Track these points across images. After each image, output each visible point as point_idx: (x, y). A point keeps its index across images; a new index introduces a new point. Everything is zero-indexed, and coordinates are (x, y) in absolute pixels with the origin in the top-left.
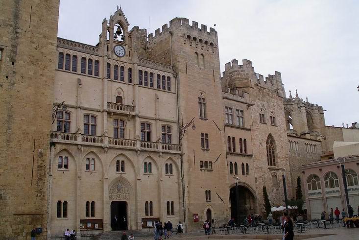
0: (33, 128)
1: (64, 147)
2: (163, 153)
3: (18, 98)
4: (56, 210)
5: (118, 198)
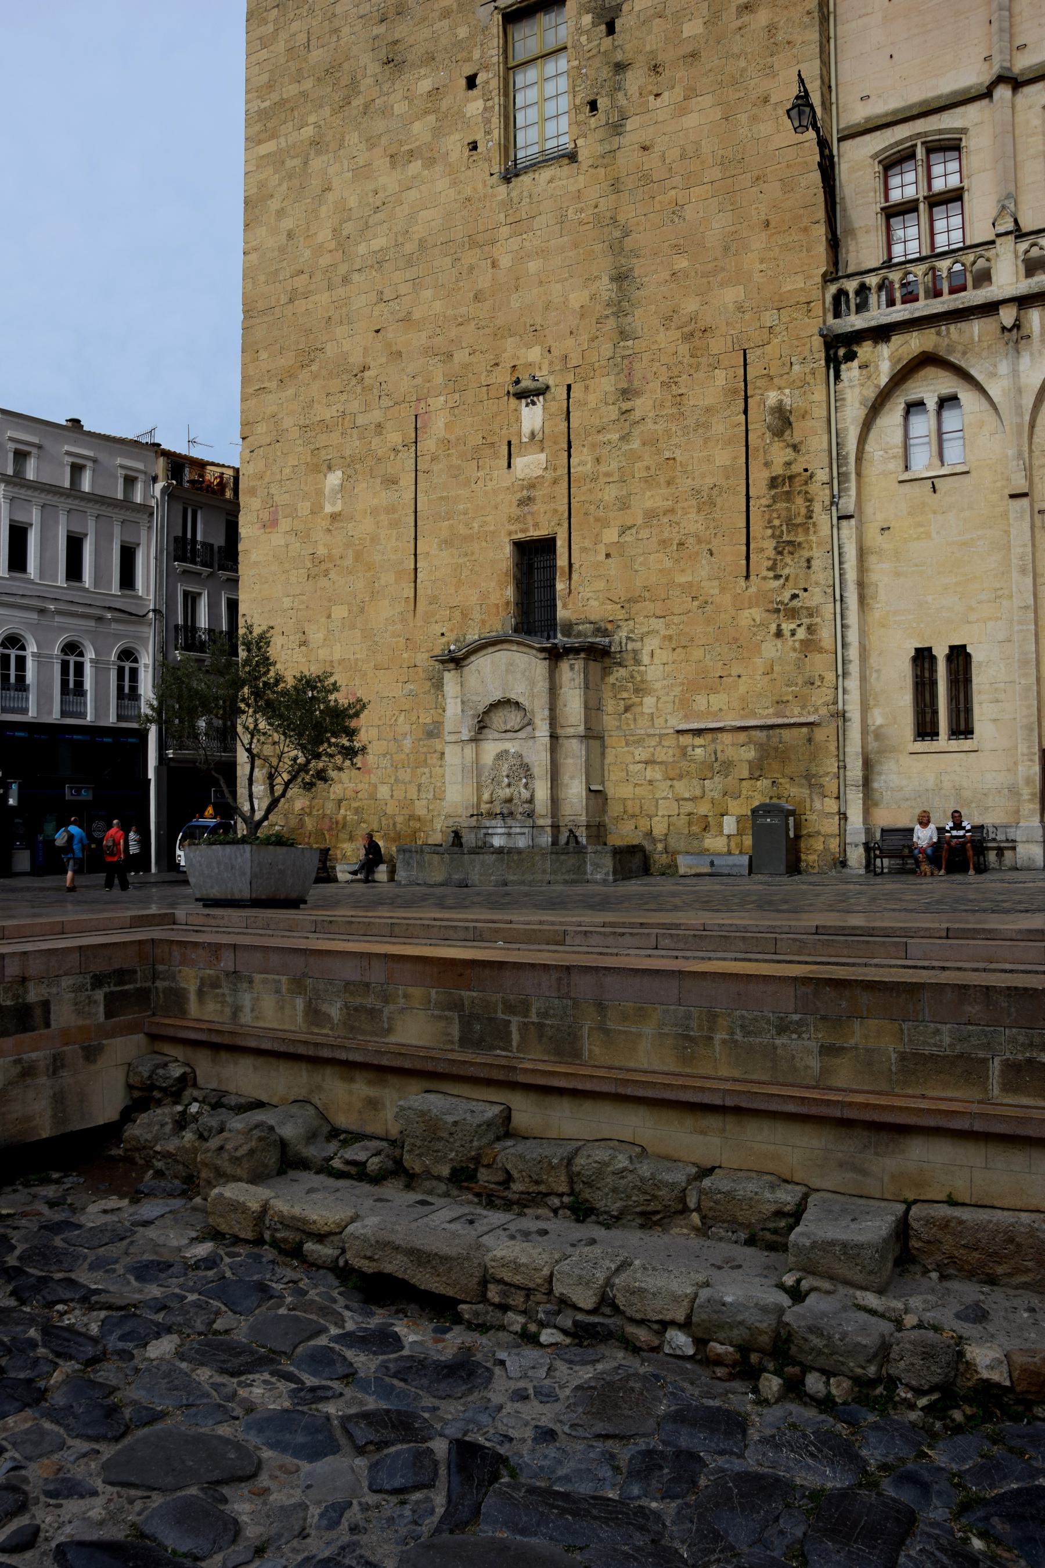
0: (731, 295)
1: (914, 343)
3: (646, 179)
4: (905, 700)
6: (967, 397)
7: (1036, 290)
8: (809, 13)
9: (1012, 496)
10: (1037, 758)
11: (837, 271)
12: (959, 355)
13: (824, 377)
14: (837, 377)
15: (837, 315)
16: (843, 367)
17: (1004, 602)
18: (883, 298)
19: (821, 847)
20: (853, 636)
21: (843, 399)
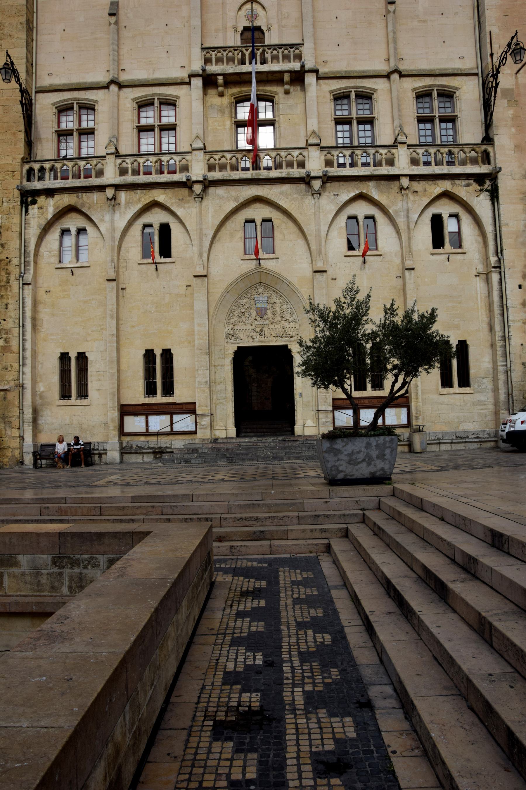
1: (66, 200)
2: (413, 177)
4: (55, 379)
5: (257, 338)
6: (90, 229)
7: (123, 183)
8: (21, 24)
9: (108, 280)
10: (116, 409)
11: (31, 158)
12: (87, 209)
13: (19, 211)
14: (27, 212)
15: (29, 180)
16: (30, 207)
17: (104, 332)
18: (52, 175)
19: (10, 455)
20: (28, 345)
21: (29, 224)
